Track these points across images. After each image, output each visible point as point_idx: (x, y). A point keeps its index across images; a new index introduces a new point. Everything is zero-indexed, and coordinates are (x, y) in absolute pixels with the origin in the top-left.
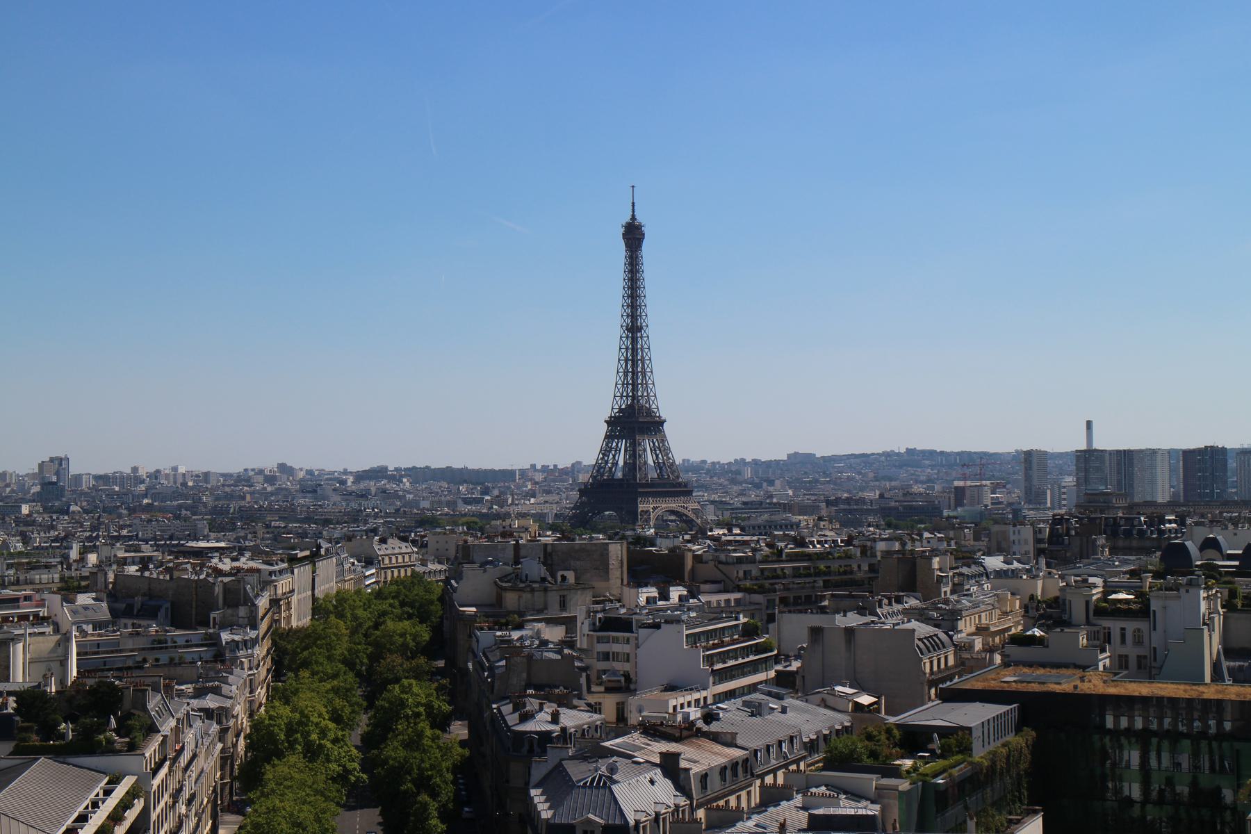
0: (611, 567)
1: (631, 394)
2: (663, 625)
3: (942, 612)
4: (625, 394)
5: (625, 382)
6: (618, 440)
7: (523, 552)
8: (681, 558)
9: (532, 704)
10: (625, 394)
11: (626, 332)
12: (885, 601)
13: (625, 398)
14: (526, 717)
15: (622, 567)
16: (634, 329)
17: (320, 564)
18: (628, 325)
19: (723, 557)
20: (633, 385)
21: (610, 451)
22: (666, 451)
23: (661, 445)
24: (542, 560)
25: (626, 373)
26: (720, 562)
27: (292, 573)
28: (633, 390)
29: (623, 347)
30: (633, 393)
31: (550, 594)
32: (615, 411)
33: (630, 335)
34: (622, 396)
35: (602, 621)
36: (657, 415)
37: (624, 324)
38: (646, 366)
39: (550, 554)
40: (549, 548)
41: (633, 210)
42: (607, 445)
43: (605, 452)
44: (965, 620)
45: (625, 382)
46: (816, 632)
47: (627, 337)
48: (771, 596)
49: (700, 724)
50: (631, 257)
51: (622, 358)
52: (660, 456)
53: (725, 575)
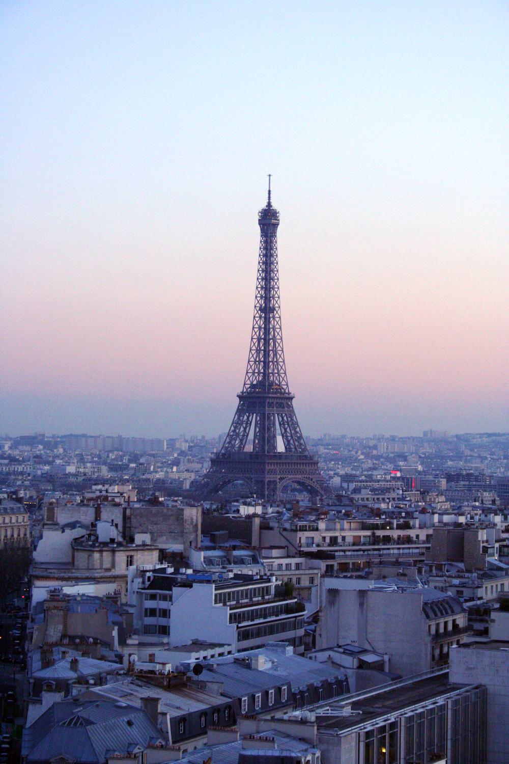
0: (185, 531)
1: (262, 371)
2: (194, 584)
3: (464, 580)
4: (256, 371)
5: (257, 360)
6: (249, 413)
9: (56, 654)
10: (256, 371)
11: (259, 312)
13: (256, 374)
15: (196, 531)
18: (261, 305)
20: (264, 362)
22: (294, 425)
23: (289, 419)
24: (119, 520)
25: (258, 351)
26: (285, 529)
28: (264, 368)
29: (256, 326)
30: (264, 371)
31: (117, 554)
32: (247, 386)
33: (263, 315)
34: (254, 373)
35: (152, 579)
36: (287, 391)
37: (258, 305)
38: (277, 345)
41: (269, 198)
42: (239, 418)
43: (237, 424)
44: (486, 587)
45: (257, 360)
47: (260, 317)
48: (330, 562)
49: (191, 674)
50: (266, 242)
51: (255, 337)
52: (288, 430)
53: (287, 540)
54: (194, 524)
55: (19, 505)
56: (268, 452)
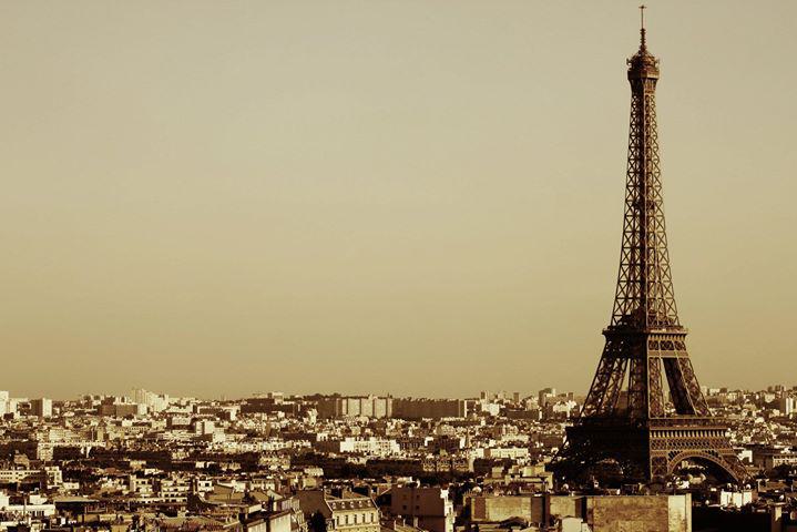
4: (630, 296)
7: (554, 510)
8: (770, 514)
10: (630, 296)
15: (686, 528)
17: (274, 523)
18: (635, 199)
20: (642, 282)
21: (609, 376)
25: (632, 265)
29: (629, 229)
30: (642, 295)
32: (618, 318)
34: (626, 298)
37: (630, 198)
42: (606, 365)
43: (604, 374)
47: (634, 216)
51: (628, 245)
54: (683, 518)
55: (366, 498)
56: (652, 416)
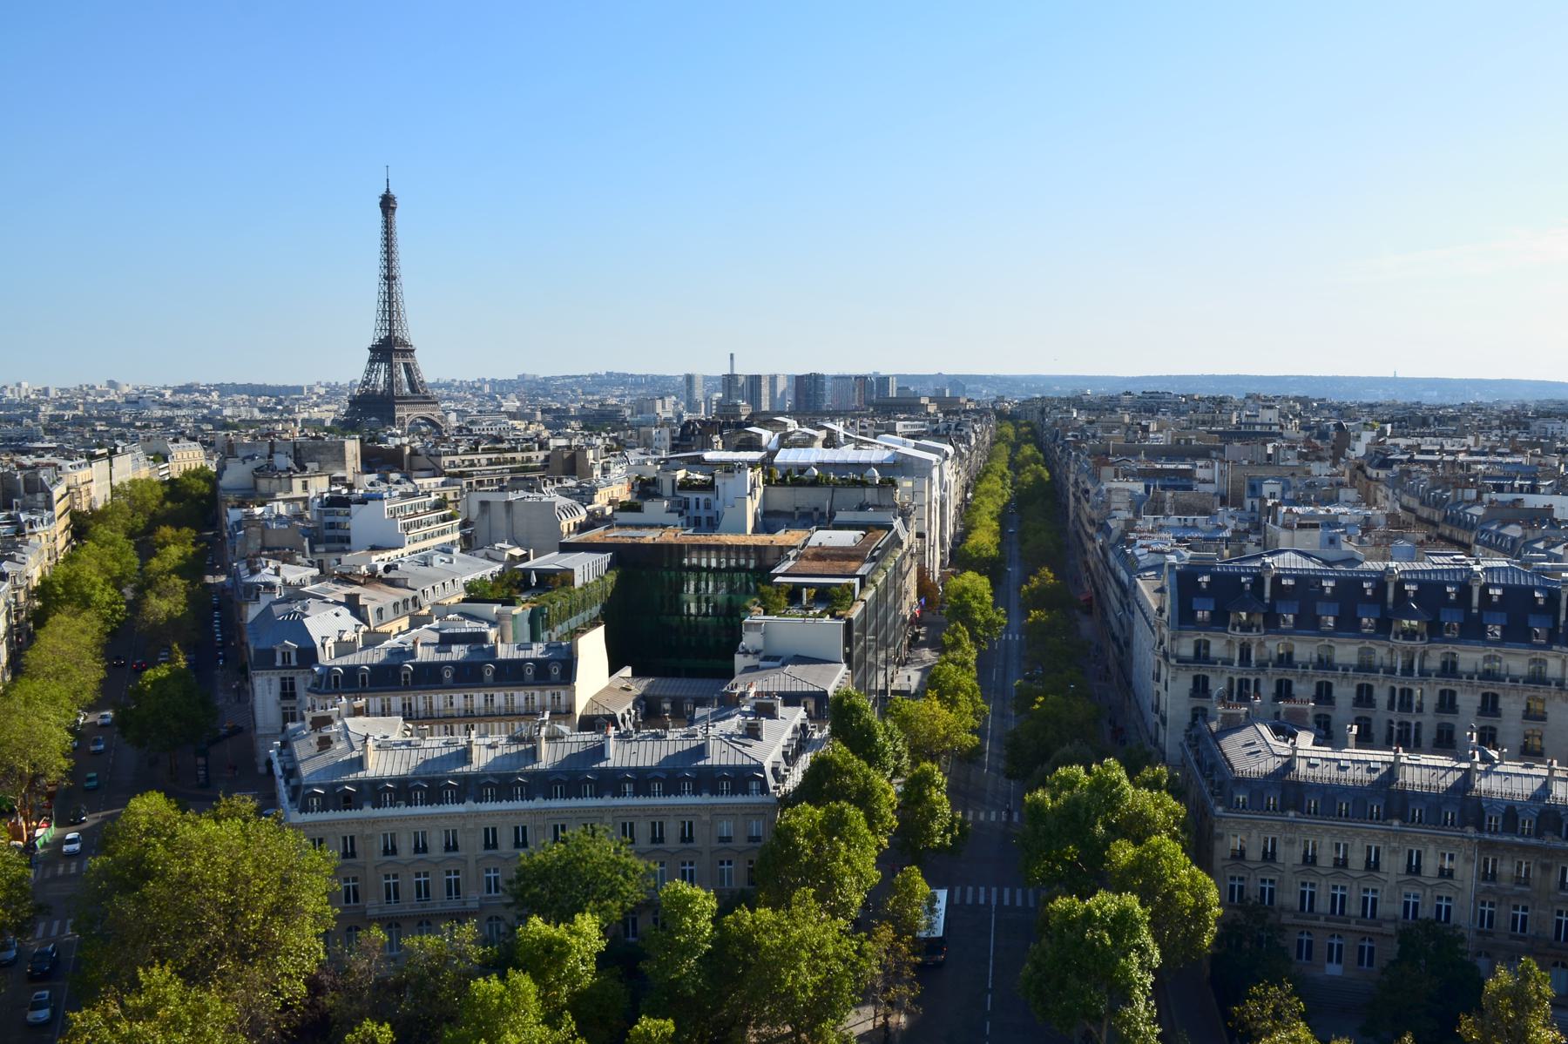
7: (277, 449)
12: (548, 482)
14: (254, 572)
16: (390, 278)
17: (116, 460)
19: (433, 452)
20: (390, 321)
24: (291, 452)
25: (384, 312)
26: (431, 455)
27: (91, 466)
28: (390, 325)
39: (299, 450)
40: (298, 446)
43: (370, 371)
46: (484, 504)
50: (386, 222)
